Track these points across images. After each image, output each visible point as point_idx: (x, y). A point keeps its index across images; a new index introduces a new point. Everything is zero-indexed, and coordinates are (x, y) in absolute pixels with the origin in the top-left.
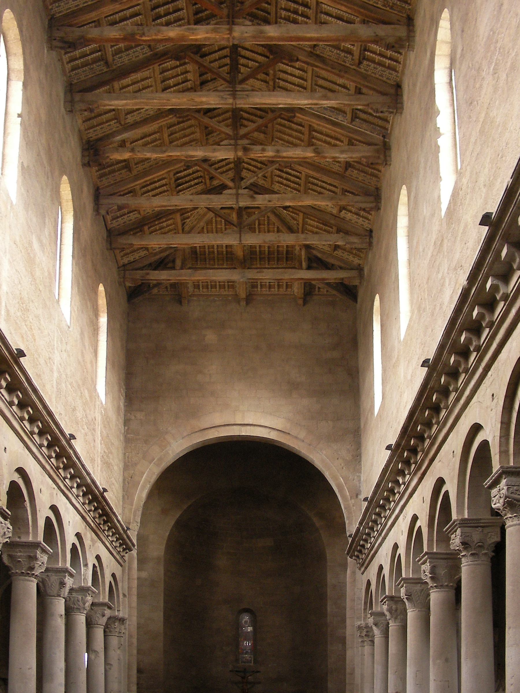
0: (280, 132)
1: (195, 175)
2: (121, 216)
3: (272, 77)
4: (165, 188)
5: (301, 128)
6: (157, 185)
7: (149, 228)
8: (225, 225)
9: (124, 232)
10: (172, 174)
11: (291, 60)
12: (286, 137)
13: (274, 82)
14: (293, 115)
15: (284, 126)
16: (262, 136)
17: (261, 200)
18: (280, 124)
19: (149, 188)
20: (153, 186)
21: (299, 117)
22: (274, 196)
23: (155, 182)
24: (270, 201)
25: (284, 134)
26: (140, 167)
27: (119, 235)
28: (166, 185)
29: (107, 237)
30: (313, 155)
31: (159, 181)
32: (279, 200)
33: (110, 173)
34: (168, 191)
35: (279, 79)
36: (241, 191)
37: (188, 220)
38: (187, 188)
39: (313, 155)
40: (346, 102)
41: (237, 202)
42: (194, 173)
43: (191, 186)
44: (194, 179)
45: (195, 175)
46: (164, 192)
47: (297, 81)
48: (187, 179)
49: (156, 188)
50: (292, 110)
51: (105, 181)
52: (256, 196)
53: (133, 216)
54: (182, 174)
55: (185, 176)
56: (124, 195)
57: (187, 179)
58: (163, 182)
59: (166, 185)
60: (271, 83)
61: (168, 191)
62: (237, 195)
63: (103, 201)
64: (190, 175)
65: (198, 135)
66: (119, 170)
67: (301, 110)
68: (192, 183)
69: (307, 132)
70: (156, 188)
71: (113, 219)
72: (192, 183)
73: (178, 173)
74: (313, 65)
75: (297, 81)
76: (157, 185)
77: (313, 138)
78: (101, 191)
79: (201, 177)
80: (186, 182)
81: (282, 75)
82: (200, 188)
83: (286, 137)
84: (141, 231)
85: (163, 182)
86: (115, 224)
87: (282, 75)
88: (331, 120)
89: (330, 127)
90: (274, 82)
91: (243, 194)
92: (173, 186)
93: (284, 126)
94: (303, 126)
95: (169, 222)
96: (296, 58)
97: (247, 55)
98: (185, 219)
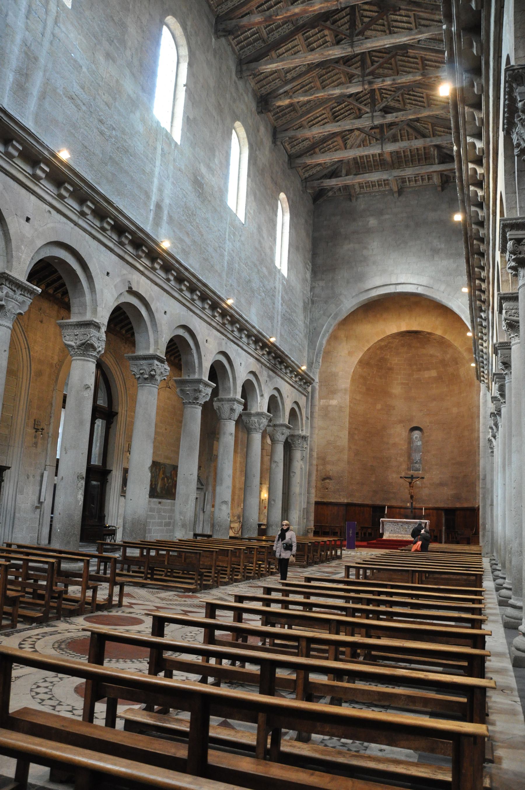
0: (402, 66)
1: (347, 108)
2: (297, 145)
3: (387, 26)
4: (326, 120)
5: (416, 60)
6: (320, 119)
7: (320, 150)
8: (370, 141)
9: (300, 156)
10: (328, 109)
11: (395, 11)
12: (408, 69)
13: (390, 30)
14: (406, 51)
15: (404, 61)
16: (390, 72)
17: (390, 118)
18: (401, 61)
19: (314, 122)
20: (317, 120)
21: (410, 52)
22: (400, 113)
23: (318, 117)
24: (396, 117)
25: (405, 67)
26: (304, 109)
27: (296, 158)
28: (326, 118)
29: (288, 160)
30: (420, 78)
31: (320, 116)
32: (403, 115)
33: (283, 115)
34: (328, 122)
35: (393, 27)
36: (375, 114)
37: (348, 141)
38: (343, 118)
39: (420, 78)
40: (436, 33)
41: (373, 121)
42: (346, 107)
43: (346, 116)
44: (347, 111)
45: (347, 108)
46: (326, 123)
47: (406, 25)
48: (342, 111)
49: (320, 121)
50: (404, 48)
51: (280, 122)
52: (385, 115)
53: (306, 144)
54: (337, 108)
55: (339, 110)
56: (297, 129)
57: (342, 111)
58: (324, 116)
59: (326, 118)
60: (388, 32)
61: (328, 122)
62: (373, 117)
63: (279, 136)
64: (343, 108)
65: (343, 79)
66: (289, 113)
67: (411, 46)
68: (346, 114)
69: (420, 63)
70: (320, 121)
71: (292, 148)
72: (346, 114)
73: (333, 108)
74: (412, 11)
75: (406, 25)
76: (320, 119)
77: (426, 66)
78: (278, 130)
79: (352, 108)
80: (341, 114)
81: (395, 24)
82: (352, 116)
83: (408, 69)
84: (314, 153)
85: (324, 116)
86: (293, 151)
87: (395, 24)
88: (435, 49)
89: (434, 54)
90: (390, 30)
91: (377, 116)
92: (332, 118)
93: (404, 61)
94: (417, 59)
95: (334, 144)
96: (398, 8)
97: (368, 15)
98: (345, 141)
